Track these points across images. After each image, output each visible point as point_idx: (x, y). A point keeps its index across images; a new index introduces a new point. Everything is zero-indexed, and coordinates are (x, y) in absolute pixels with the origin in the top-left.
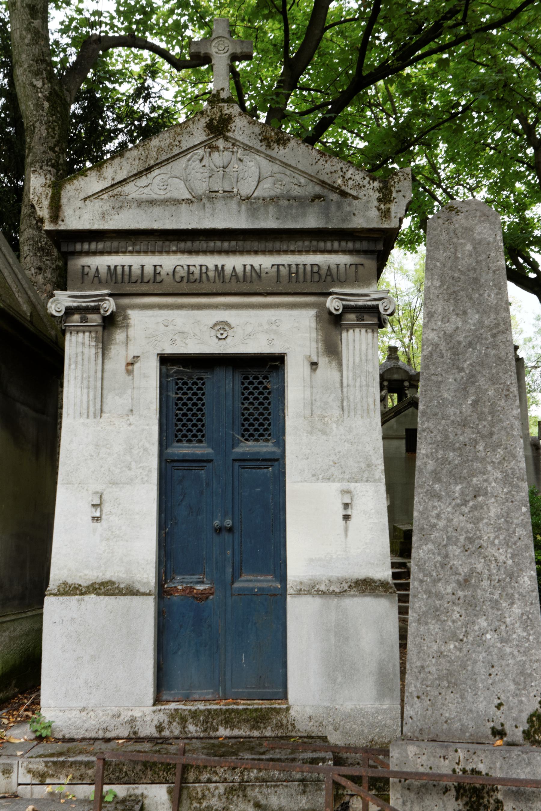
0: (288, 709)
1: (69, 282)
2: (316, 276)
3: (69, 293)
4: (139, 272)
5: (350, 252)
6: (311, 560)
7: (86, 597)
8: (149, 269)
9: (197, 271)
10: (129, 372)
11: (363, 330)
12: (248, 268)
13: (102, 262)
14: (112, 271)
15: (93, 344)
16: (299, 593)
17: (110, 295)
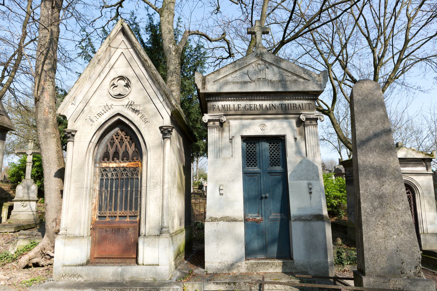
0: (293, 262)
1: (208, 111)
2: (295, 108)
3: (208, 114)
4: (233, 107)
5: (308, 99)
6: (299, 208)
7: (220, 222)
8: (236, 106)
9: (253, 106)
10: (231, 142)
11: (312, 127)
12: (271, 105)
13: (220, 104)
14: (223, 107)
15: (218, 132)
16: (295, 220)
17: (224, 115)
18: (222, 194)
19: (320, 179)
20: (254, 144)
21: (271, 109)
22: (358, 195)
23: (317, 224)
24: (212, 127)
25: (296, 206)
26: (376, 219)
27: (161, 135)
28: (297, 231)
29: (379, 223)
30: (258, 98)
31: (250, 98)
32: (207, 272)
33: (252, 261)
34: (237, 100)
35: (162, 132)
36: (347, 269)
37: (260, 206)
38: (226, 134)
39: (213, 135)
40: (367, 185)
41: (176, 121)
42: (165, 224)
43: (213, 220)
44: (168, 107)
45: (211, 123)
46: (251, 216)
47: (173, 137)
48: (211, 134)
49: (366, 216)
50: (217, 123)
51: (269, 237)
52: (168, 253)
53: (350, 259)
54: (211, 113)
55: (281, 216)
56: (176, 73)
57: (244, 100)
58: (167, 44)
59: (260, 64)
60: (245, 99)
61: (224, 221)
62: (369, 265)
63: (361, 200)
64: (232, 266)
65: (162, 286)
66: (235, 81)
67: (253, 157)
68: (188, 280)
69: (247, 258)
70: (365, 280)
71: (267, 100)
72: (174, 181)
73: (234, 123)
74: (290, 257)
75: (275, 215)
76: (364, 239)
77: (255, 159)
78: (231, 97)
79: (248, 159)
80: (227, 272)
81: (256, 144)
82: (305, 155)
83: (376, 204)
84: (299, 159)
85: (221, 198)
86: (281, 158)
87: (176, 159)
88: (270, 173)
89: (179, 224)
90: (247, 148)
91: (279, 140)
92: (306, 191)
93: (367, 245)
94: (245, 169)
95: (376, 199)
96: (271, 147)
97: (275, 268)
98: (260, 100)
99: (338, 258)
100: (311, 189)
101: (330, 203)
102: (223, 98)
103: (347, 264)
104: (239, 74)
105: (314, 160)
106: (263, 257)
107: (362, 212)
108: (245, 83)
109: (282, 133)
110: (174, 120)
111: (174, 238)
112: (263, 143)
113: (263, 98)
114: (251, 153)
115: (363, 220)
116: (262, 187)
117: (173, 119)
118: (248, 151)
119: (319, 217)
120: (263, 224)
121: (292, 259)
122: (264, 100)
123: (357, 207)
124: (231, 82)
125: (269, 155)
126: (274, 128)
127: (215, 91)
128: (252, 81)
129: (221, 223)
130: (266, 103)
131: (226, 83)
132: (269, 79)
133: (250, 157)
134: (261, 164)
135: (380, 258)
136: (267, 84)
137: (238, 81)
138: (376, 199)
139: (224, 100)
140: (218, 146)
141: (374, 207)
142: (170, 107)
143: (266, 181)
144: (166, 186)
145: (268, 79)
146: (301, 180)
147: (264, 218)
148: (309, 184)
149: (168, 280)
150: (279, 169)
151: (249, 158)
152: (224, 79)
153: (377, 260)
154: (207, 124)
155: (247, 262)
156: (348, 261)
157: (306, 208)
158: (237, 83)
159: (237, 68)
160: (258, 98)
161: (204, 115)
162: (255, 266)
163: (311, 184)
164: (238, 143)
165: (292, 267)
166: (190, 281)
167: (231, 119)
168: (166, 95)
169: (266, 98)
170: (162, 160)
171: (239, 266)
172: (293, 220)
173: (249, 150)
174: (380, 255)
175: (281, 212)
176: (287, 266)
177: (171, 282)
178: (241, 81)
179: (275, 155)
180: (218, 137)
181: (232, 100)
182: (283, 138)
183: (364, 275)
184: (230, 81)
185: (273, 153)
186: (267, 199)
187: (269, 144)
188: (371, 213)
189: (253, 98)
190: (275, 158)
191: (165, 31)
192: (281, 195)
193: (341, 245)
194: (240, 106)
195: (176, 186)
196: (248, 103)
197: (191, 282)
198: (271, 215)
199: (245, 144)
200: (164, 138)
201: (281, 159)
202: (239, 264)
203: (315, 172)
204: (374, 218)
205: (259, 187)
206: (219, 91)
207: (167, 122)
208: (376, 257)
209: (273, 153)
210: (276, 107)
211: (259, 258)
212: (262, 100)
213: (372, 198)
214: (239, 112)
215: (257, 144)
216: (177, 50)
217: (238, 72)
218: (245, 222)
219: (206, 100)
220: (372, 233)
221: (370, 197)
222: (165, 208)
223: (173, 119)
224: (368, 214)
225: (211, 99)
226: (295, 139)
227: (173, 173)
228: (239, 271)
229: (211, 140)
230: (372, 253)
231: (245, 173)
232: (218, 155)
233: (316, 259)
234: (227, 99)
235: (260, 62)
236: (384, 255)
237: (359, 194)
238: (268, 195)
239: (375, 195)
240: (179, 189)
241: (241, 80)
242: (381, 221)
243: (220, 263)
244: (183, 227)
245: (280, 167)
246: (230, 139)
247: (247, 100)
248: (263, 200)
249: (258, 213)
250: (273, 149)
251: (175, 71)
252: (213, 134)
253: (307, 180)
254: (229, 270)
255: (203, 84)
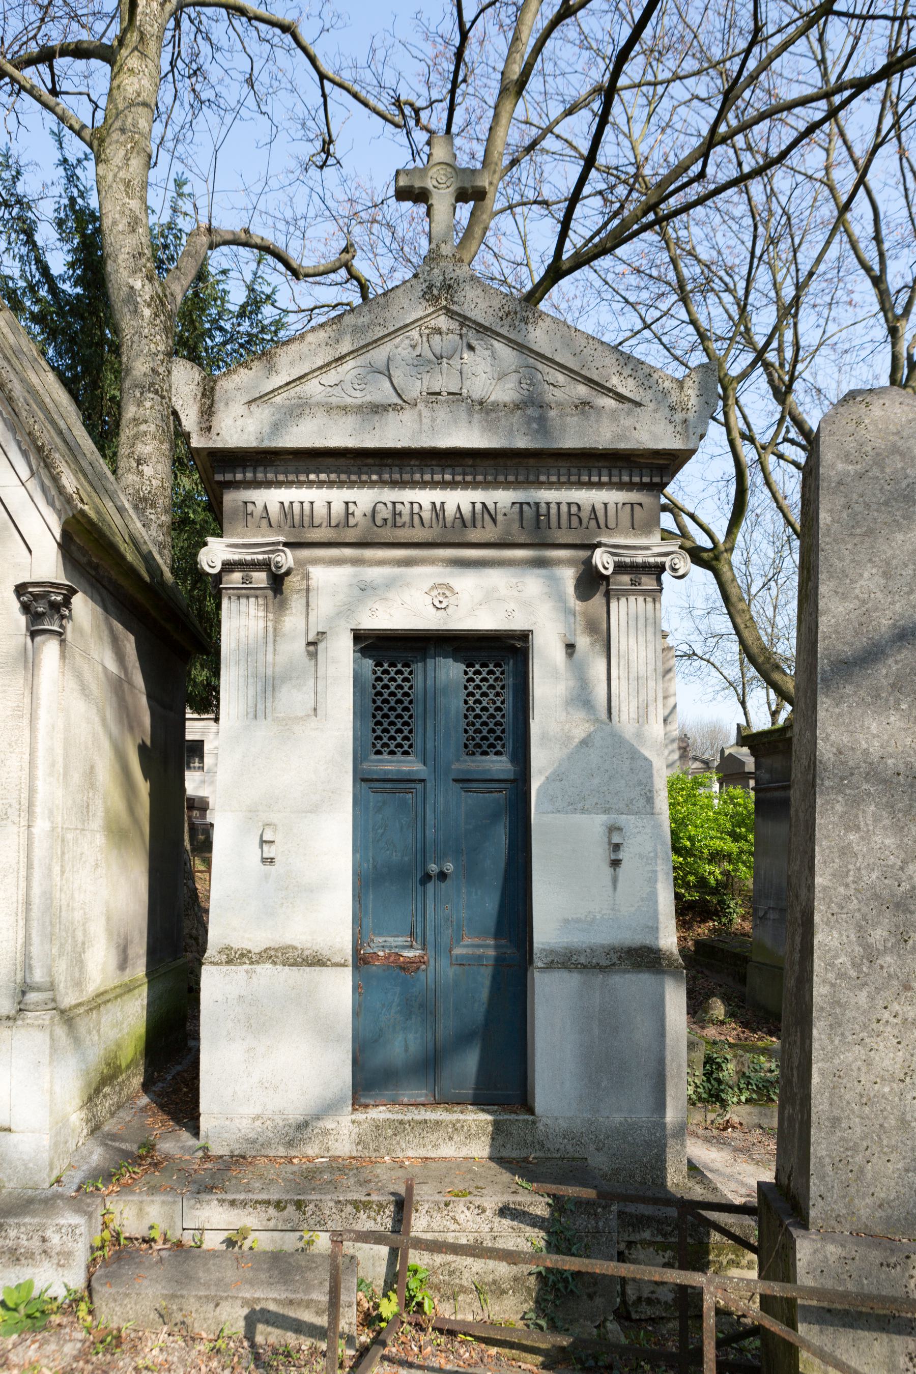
0: (534, 1122)
1: (225, 525)
2: (575, 520)
3: (226, 540)
4: (325, 511)
5: (629, 486)
6: (566, 921)
7: (258, 968)
8: (338, 509)
9: (406, 510)
10: (313, 655)
11: (641, 599)
12: (479, 507)
13: (272, 498)
14: (286, 511)
15: (261, 614)
16: (550, 966)
17: (286, 544)
18: (271, 861)
19: (657, 810)
20: (406, 665)
21: (479, 524)
22: (803, 892)
23: (631, 985)
24: (245, 593)
25: (555, 915)
26: (871, 997)
27: (22, 620)
28: (554, 1004)
29: (886, 1015)
30: (427, 477)
31: (397, 477)
32: (205, 1149)
33: (379, 1113)
34: (341, 484)
35: (26, 608)
36: (736, 1119)
37: (420, 906)
38: (293, 620)
39: (240, 624)
40: (845, 851)
41: (96, 567)
42: (38, 976)
43: (236, 957)
44: (51, 503)
45: (237, 576)
46: (384, 944)
47: (79, 631)
48: (235, 623)
49: (833, 985)
50: (260, 578)
51: (447, 1026)
52: (47, 1086)
53: (749, 1084)
54: (238, 535)
55: (497, 947)
56: (156, 392)
57: (372, 484)
58: (124, 273)
59: (439, 332)
60: (374, 477)
61: (274, 963)
62: (823, 1193)
63: (817, 918)
64: (303, 1127)
65: (16, 1215)
66: (334, 400)
67: (400, 716)
68: (127, 1185)
69: (363, 1100)
70: (806, 1250)
71: (465, 485)
72: (85, 810)
73: (328, 580)
74: (525, 1103)
75: (477, 946)
76: (816, 1079)
77: (406, 724)
78: (318, 472)
79: (378, 723)
80: (282, 1151)
81: (414, 667)
82: (604, 715)
83: (878, 935)
84: (580, 731)
85: (266, 877)
86: (508, 721)
87: (97, 720)
88: (464, 781)
89: (112, 962)
90: (379, 679)
91: (503, 653)
92: (599, 854)
93: (826, 1106)
94: (365, 766)
95: (880, 912)
96: (471, 680)
97: (463, 1137)
98: (433, 485)
99: (709, 1081)
100: (617, 847)
101: (695, 874)
102: (286, 473)
103: (739, 1102)
104: (354, 372)
105: (639, 735)
106: (422, 1100)
107: (818, 965)
108: (377, 409)
109: (517, 624)
110: (84, 560)
111: (82, 1026)
112: (441, 661)
113: (448, 477)
114: (393, 700)
115: (817, 999)
116: (430, 832)
117: (77, 555)
118: (379, 694)
119: (645, 958)
120: (426, 977)
121: (531, 1111)
122: (452, 485)
123: (798, 939)
124: (318, 404)
125: (463, 707)
126: (490, 598)
127: (254, 444)
128: (402, 403)
129: (265, 969)
130: (458, 500)
131: (298, 410)
132: (476, 396)
133: (386, 716)
134: (430, 745)
135: (874, 1160)
136: (464, 415)
137: (349, 400)
138: (880, 912)
139: (288, 484)
140: (261, 670)
141: (867, 947)
142: (57, 504)
143: (448, 806)
144: (41, 826)
145: (466, 397)
146: (583, 811)
147: (431, 952)
148: (613, 829)
149: (47, 1185)
150: (499, 765)
151: (386, 717)
152: (292, 393)
153: (861, 1170)
154: (218, 578)
155: (360, 1116)
156: (740, 1090)
157: (594, 918)
158: (345, 409)
159: (346, 347)
160: (427, 477)
161: (205, 544)
162: (390, 1132)
163: (619, 829)
164: (342, 656)
165: (529, 1139)
166: (133, 1192)
167: (315, 562)
168: (40, 449)
169: (459, 478)
170: (26, 721)
171: (326, 1132)
172: (540, 964)
173: (386, 687)
174: (875, 1148)
175: (498, 935)
176: (509, 1134)
177: (57, 1196)
178: (358, 402)
179: (484, 709)
180: (261, 633)
181: (320, 484)
182: (518, 645)
183: (804, 1225)
184: (313, 400)
185: (477, 702)
186: (448, 881)
187: (463, 667)
188: (854, 974)
189: (406, 477)
190: (485, 724)
191: (115, 223)
192: (502, 865)
193: (722, 1023)
194: (352, 507)
195: (97, 823)
196: (389, 495)
197: (135, 1198)
198: (458, 942)
199: (369, 663)
200: (33, 634)
201: (504, 726)
202: (329, 1124)
203: (640, 783)
204: (864, 994)
205: (420, 836)
206: (266, 444)
207: (47, 565)
208: (859, 1159)
209: (477, 702)
210: (500, 518)
211: (406, 1100)
212: (444, 485)
213: (865, 910)
214: (351, 535)
215: (418, 667)
216: (159, 302)
217: (351, 364)
218: (356, 967)
219: (215, 476)
220: (852, 1056)
221: (854, 905)
222: (35, 913)
223: (77, 555)
224: (841, 975)
225: (239, 477)
226: (570, 648)
227: (76, 777)
228: (328, 1150)
229: (233, 645)
230: (842, 1139)
231: (363, 780)
232: (260, 707)
233: (620, 1112)
234: (302, 478)
235: (442, 322)
236: (894, 1148)
237: (811, 887)
238: (449, 867)
239: (877, 896)
240: (117, 834)
241: (358, 397)
242: (896, 1007)
243: (257, 1118)
244: (139, 970)
245: (504, 758)
246: (309, 644)
247: (382, 483)
248: (430, 886)
249: (412, 934)
250: (478, 687)
251: (152, 384)
252: (243, 621)
253: (606, 811)
254: (290, 1144)
255: (202, 413)
